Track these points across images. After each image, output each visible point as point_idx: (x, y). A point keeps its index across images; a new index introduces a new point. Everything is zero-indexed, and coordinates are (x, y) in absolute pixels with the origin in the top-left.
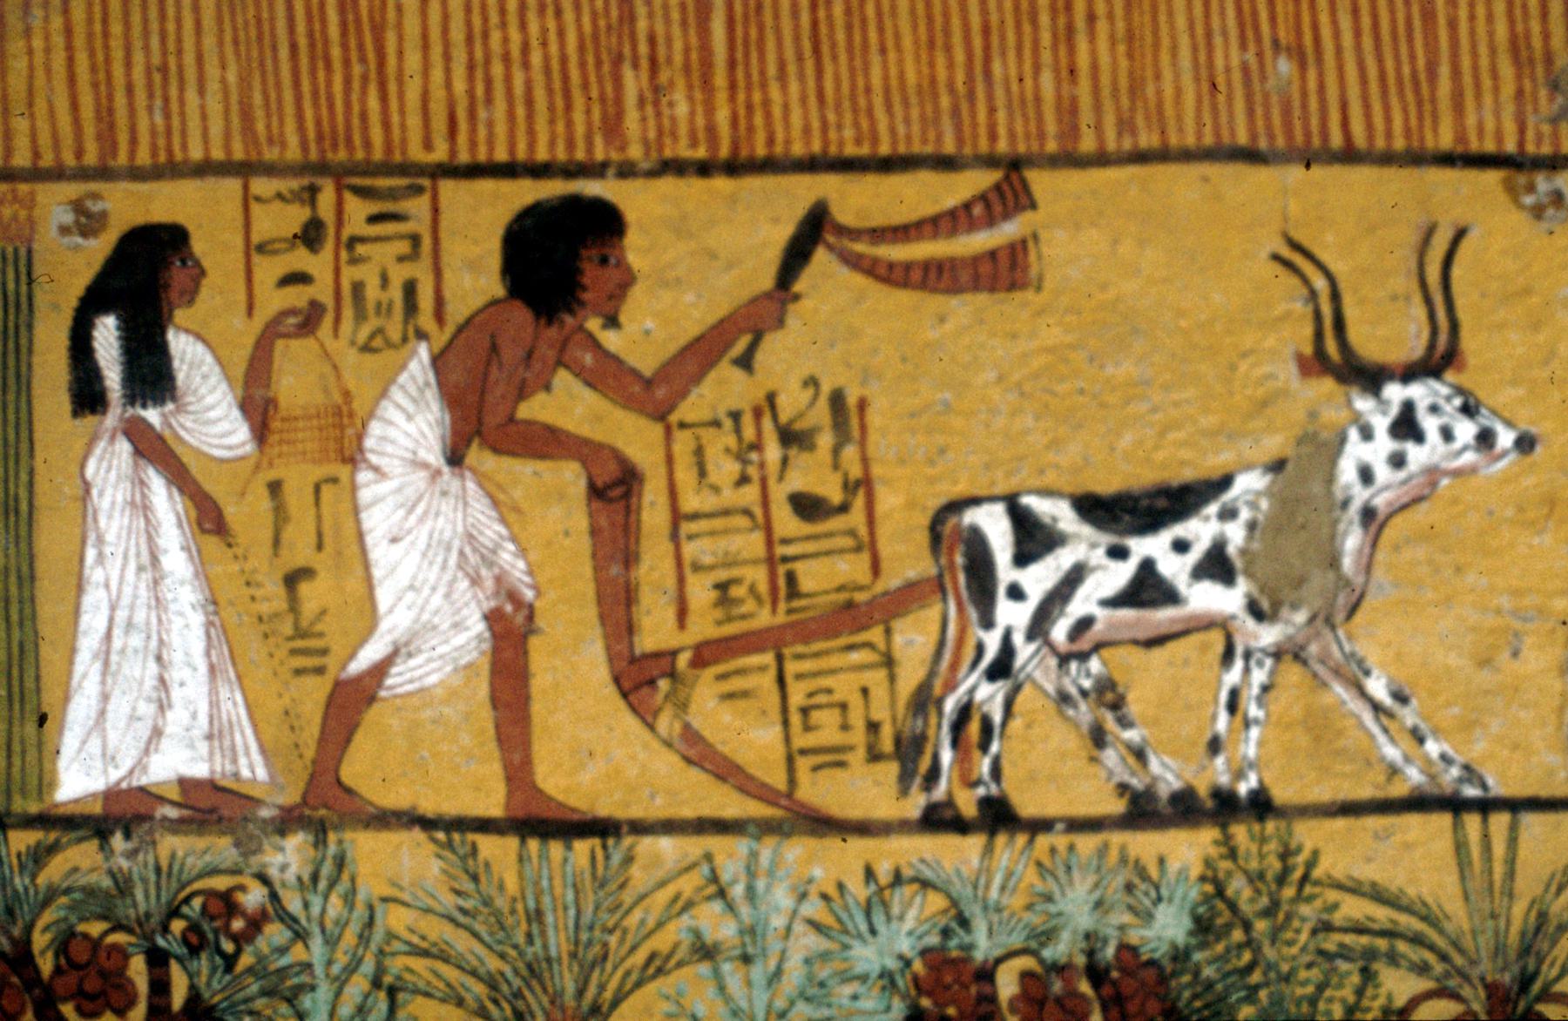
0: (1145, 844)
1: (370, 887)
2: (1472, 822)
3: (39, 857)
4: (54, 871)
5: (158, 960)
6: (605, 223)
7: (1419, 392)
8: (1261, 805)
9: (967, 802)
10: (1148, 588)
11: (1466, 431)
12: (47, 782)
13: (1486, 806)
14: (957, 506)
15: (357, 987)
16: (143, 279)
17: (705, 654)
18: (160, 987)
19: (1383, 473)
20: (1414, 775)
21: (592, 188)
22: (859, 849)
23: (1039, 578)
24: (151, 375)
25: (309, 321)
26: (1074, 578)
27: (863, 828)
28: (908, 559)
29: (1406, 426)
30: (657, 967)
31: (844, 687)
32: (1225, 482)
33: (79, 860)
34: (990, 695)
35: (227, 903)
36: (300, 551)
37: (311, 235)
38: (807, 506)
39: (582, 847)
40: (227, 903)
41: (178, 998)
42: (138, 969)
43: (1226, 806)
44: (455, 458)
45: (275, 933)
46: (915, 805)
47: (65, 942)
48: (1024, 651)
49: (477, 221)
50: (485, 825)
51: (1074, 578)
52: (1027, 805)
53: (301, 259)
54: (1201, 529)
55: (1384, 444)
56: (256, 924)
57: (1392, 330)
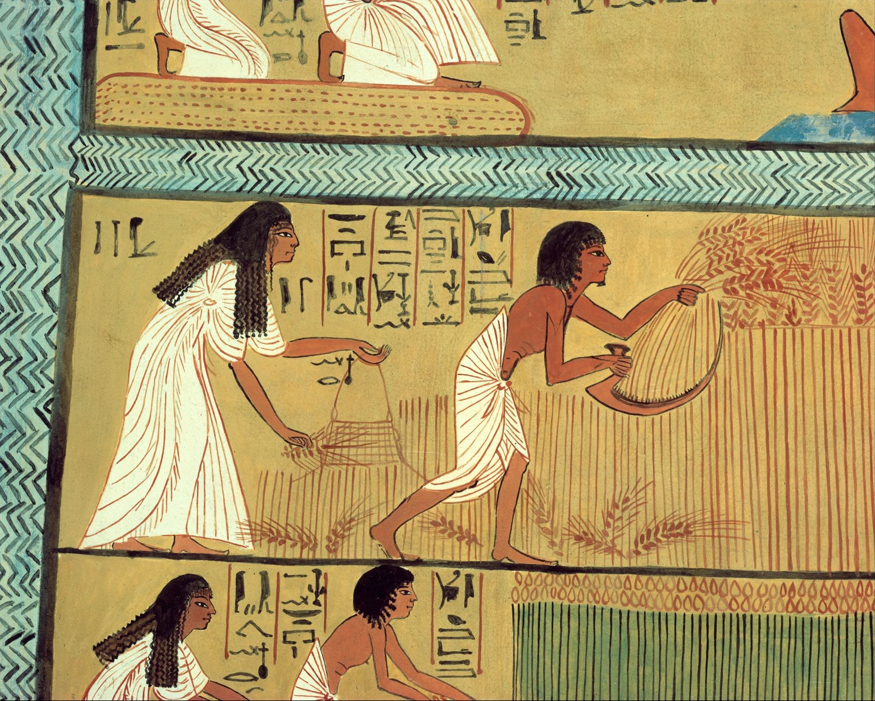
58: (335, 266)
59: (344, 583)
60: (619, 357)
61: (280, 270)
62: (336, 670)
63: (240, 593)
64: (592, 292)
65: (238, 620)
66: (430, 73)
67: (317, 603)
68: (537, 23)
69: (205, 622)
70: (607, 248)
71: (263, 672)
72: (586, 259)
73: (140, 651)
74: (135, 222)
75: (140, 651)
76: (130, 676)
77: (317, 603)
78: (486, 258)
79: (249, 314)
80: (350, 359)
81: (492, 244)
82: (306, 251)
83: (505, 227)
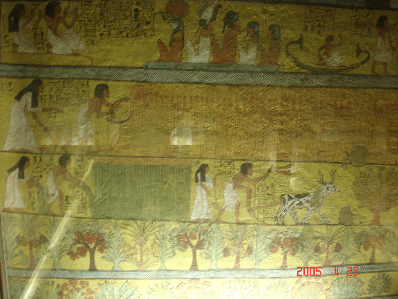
0: (297, 227)
1: (222, 229)
2: (328, 227)
3: (188, 225)
4: (190, 226)
5: (200, 235)
6: (251, 166)
7: (330, 186)
8: (308, 224)
9: (280, 223)
10: (301, 203)
11: (333, 189)
12: (190, 218)
13: (330, 225)
14: (283, 195)
15: (220, 238)
16: (203, 169)
17: (257, 208)
18: (200, 238)
19: (325, 193)
20: (323, 222)
21: (250, 162)
22: (269, 227)
23: (290, 202)
24: (203, 179)
25: (220, 174)
26: (294, 202)
27: (269, 225)
28: (277, 200)
29: (328, 189)
30: (249, 237)
31: (270, 211)
32: (309, 194)
33: (193, 226)
34: (284, 213)
35: (207, 230)
36: (217, 197)
37: (221, 166)
38: (268, 194)
39: (243, 226)
40: (207, 230)
41: (201, 239)
42: (198, 236)
43: (305, 224)
44: (234, 188)
45: (212, 233)
46: (275, 223)
47: (191, 233)
48: (288, 209)
49: (238, 165)
50: (234, 223)
51: (294, 202)
52: (286, 223)
53: (219, 168)
54: (307, 198)
55: (325, 190)
56: (210, 232)
57: (327, 179)
58: (52, 93)
59: (56, 158)
60: (112, 112)
61: (41, 94)
62: (56, 176)
63: (35, 161)
64: (106, 99)
65: (36, 166)
66: (70, 52)
67: (51, 162)
68: (93, 41)
69: (28, 166)
70: (109, 90)
71: (41, 176)
72: (105, 92)
73: (16, 171)
74: (10, 84)
75: (16, 171)
76: (15, 176)
77: (51, 162)
78: (83, 91)
79: (35, 103)
80: (55, 112)
81: (85, 89)
82: (46, 91)
83: (87, 85)
